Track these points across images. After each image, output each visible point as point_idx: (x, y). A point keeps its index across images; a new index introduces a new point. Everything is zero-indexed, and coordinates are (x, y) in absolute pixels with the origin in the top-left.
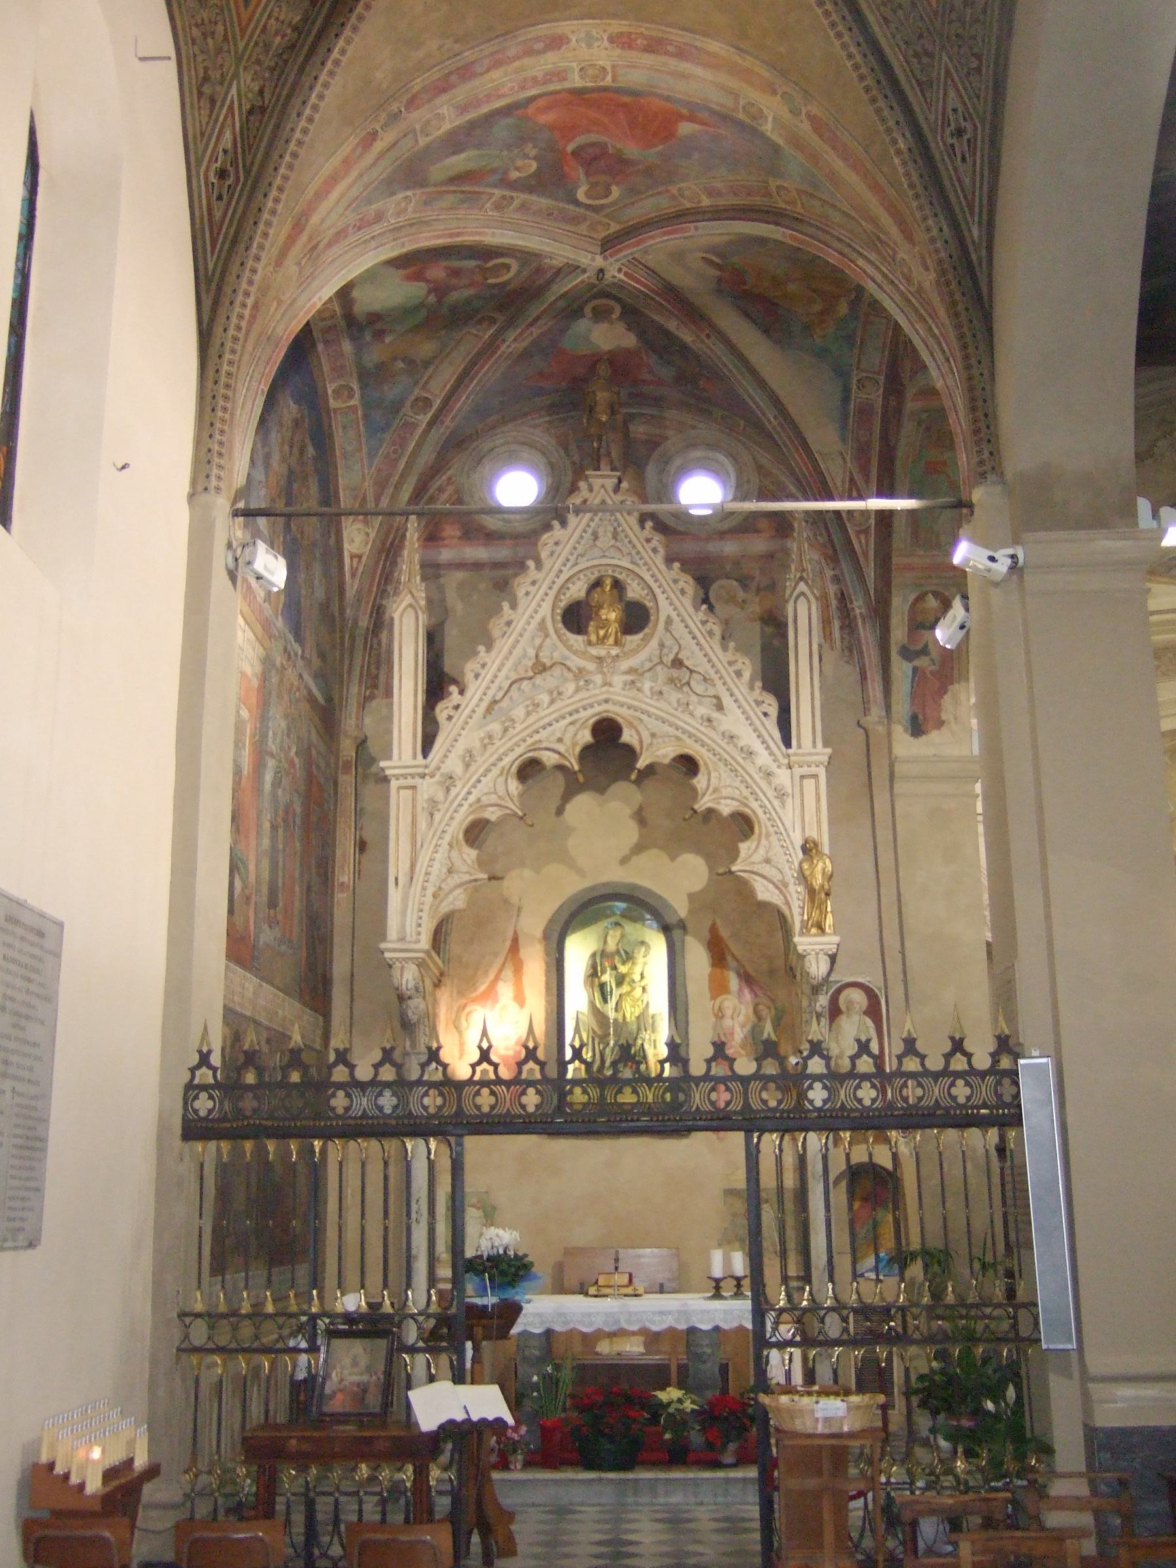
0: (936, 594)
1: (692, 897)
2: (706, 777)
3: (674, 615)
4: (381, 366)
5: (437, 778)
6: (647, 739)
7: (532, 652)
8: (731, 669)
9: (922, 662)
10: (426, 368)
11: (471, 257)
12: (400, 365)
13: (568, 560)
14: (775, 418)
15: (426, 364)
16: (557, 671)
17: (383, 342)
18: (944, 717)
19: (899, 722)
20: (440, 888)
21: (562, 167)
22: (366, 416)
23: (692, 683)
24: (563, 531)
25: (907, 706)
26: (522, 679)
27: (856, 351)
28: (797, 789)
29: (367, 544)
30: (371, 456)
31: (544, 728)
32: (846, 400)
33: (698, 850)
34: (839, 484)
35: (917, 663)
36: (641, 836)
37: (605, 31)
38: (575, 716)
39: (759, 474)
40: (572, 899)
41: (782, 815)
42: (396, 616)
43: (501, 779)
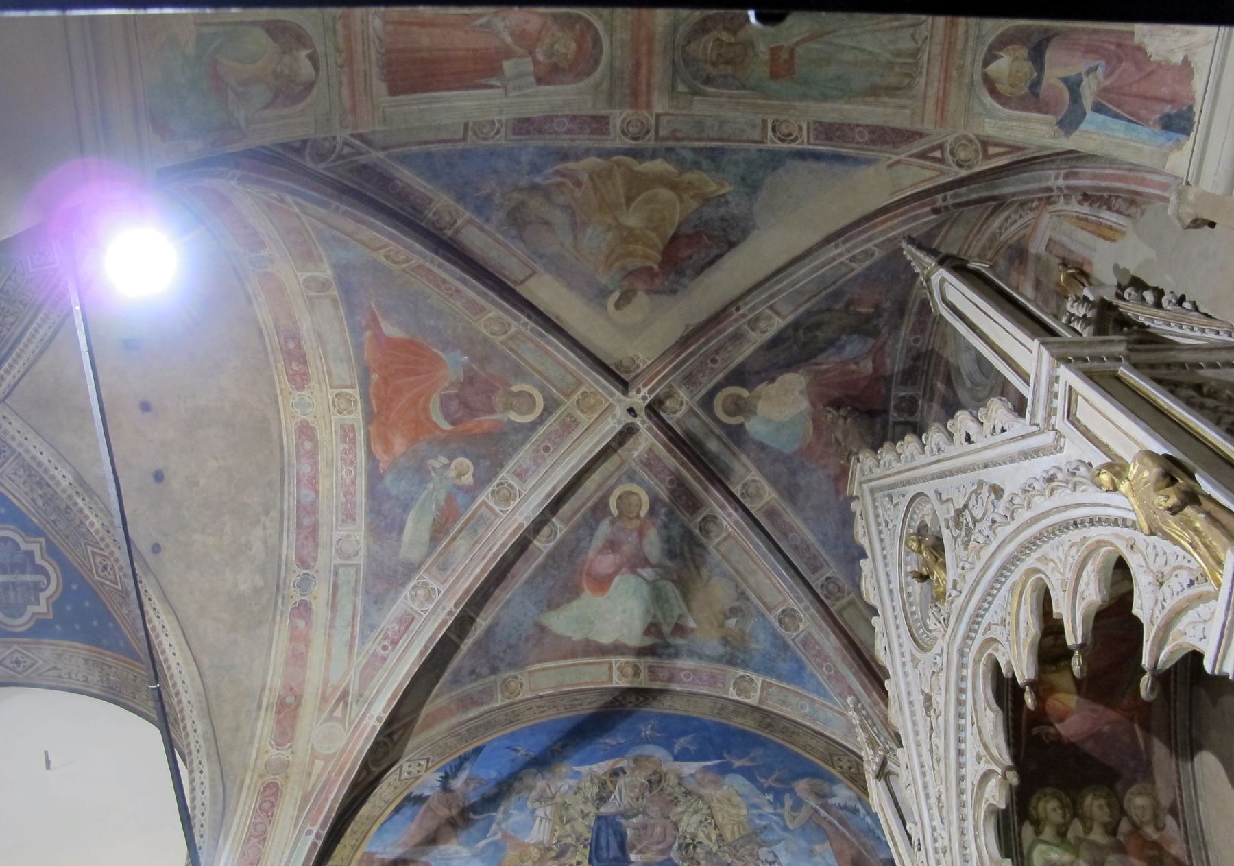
0: (990, 58)
4: (725, 641)
10: (747, 599)
11: (592, 529)
12: (732, 622)
14: (837, 246)
15: (742, 595)
17: (693, 630)
18: (1177, 59)
19: (1166, 156)
21: (475, 435)
22: (779, 677)
25: (1144, 132)
27: (734, 145)
30: (824, 694)
32: (817, 156)
34: (927, 174)
37: (290, 393)
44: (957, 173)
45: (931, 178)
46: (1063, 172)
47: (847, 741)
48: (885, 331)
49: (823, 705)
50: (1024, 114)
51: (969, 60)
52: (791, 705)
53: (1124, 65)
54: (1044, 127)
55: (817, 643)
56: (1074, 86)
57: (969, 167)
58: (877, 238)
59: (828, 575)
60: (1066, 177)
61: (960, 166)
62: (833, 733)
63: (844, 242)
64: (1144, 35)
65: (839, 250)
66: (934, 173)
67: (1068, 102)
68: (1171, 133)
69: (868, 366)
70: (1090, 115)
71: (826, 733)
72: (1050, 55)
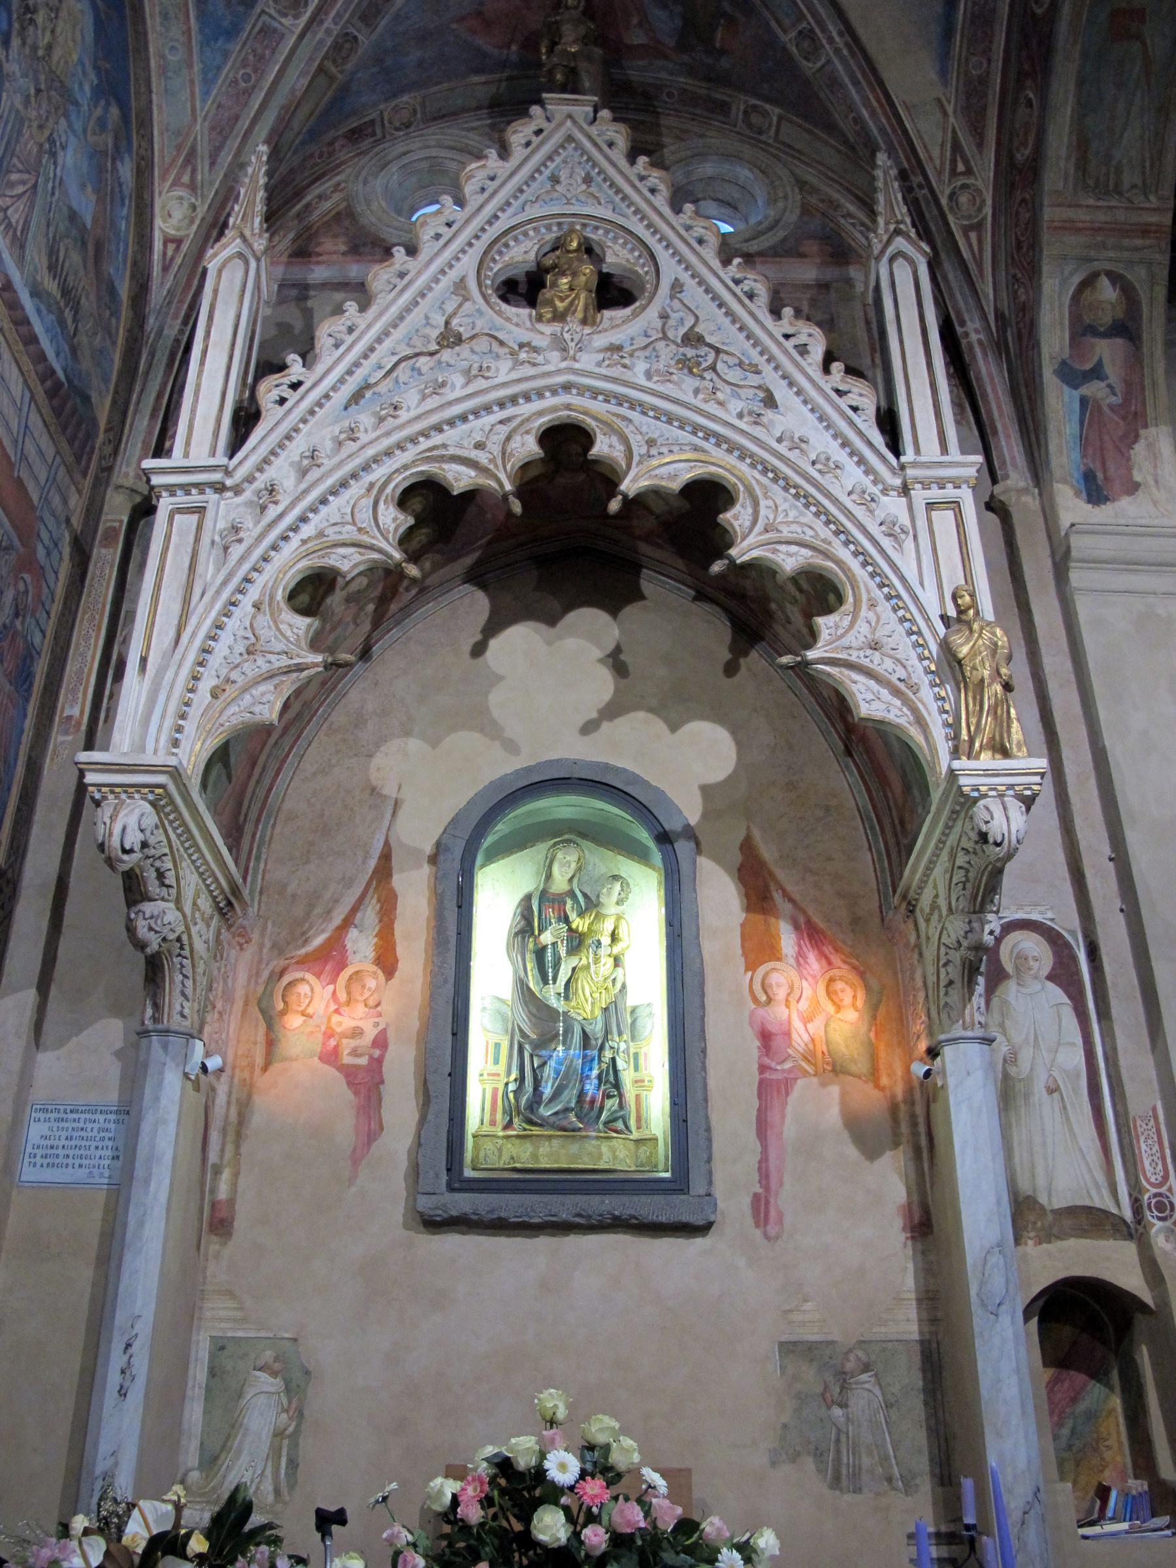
0: (1114, 277)
1: (706, 790)
2: (750, 510)
3: (685, 277)
5: (248, 494)
6: (639, 449)
7: (440, 320)
8: (789, 344)
9: (1094, 389)
13: (508, 204)
14: (841, 34)
16: (482, 344)
18: (1137, 477)
19: (1064, 481)
20: (228, 680)
23: (720, 366)
24: (501, 163)
25: (1076, 455)
26: (417, 355)
28: (922, 523)
29: (192, 222)
30: (208, 82)
31: (451, 423)
33: (718, 715)
34: (936, 153)
35: (1089, 389)
36: (617, 691)
38: (510, 411)
39: (801, 189)
40: (493, 786)
41: (899, 563)
42: (212, 266)
43: (368, 502)
44: (942, 192)
45: (931, 158)
46: (982, 337)
47: (161, 134)
48: (686, 58)
49: (192, 82)
50: (1067, 322)
51: (1111, 254)
52: (168, 30)
53: (1122, 423)
54: (1058, 345)
55: (273, 52)
56: (1097, 373)
57: (951, 209)
58: (858, 92)
59: (360, 37)
60: (980, 342)
61: (952, 196)
62: (160, 107)
63: (847, 44)
64: (1146, 439)
65: (837, 39)
66: (938, 162)
67: (1082, 368)
68: (1082, 482)
69: (637, 38)
70: (1076, 394)
71: (154, 97)
72: (1119, 341)
